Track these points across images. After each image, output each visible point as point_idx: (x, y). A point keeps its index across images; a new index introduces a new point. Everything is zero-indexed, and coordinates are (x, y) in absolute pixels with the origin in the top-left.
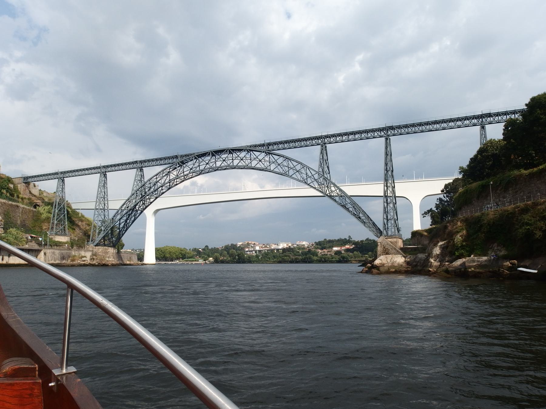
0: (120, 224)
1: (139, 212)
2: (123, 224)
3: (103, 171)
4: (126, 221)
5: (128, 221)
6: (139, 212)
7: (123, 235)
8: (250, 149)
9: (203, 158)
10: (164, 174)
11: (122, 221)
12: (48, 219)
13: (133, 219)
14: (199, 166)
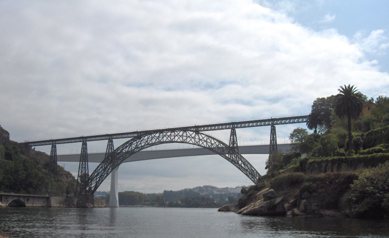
1: (110, 170)
3: (84, 140)
4: (101, 176)
6: (110, 170)
8: (185, 129)
9: (154, 134)
10: (127, 145)
11: (98, 176)
13: (106, 175)
14: (152, 140)
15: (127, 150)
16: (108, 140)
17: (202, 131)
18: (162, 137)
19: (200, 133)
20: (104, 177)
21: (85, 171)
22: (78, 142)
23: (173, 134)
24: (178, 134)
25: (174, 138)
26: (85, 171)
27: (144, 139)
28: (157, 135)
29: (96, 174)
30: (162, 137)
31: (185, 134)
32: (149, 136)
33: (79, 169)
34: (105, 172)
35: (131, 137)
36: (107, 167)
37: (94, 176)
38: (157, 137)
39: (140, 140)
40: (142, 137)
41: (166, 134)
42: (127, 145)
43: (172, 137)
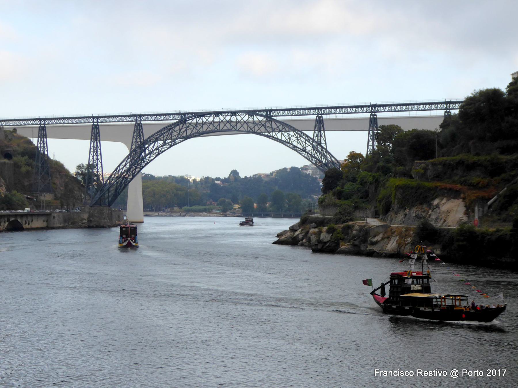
7: (119, 194)
9: (207, 118)
12: (28, 173)
17: (275, 116)
39: (185, 126)
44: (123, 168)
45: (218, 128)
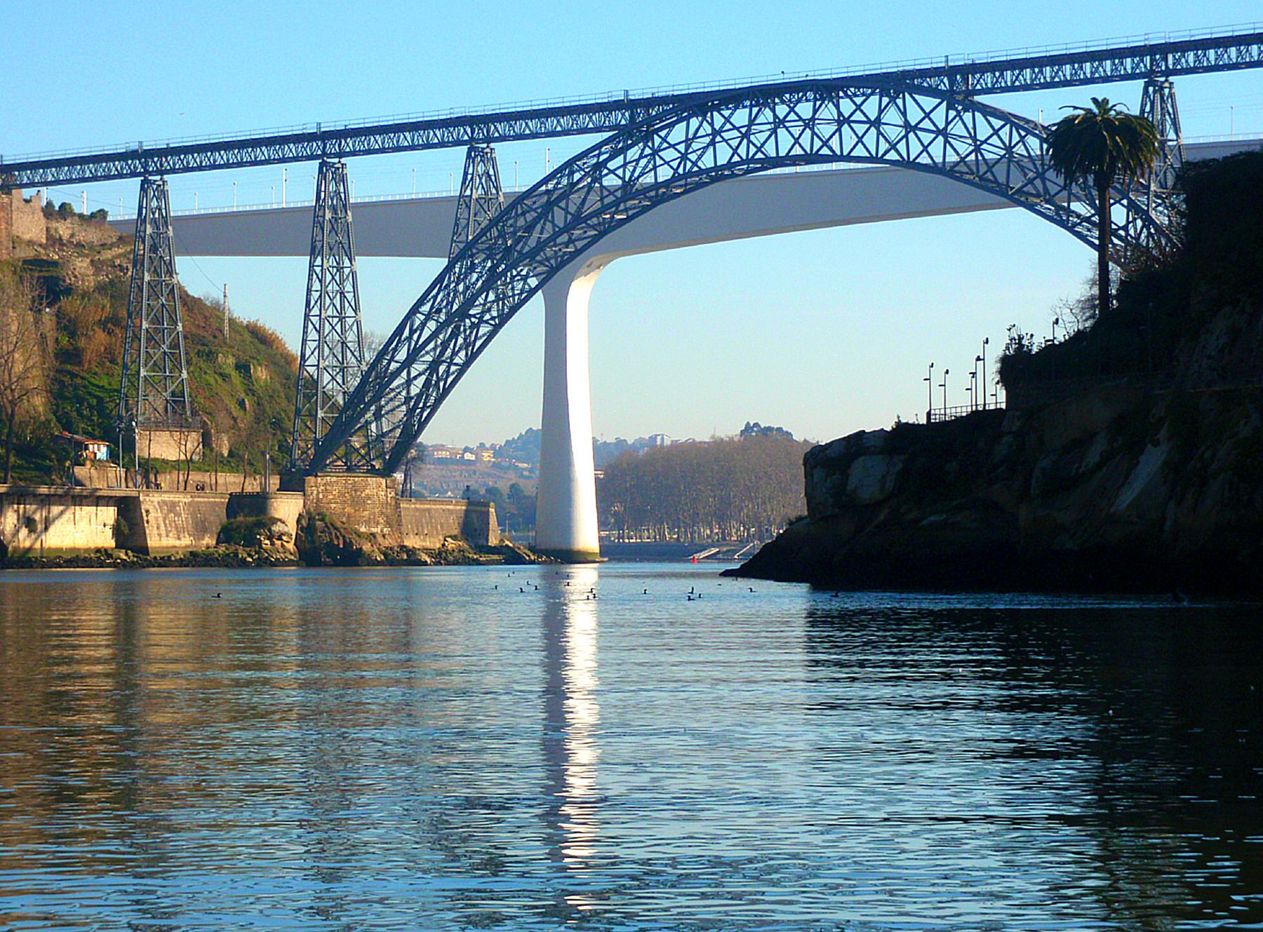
0: (409, 382)
1: (484, 329)
2: (420, 382)
5: (442, 368)
6: (484, 329)
7: (422, 425)
8: (894, 84)
9: (726, 113)
10: (577, 176)
11: (417, 368)
13: (461, 358)
14: (713, 143)
15: (572, 209)
16: (465, 148)
18: (769, 127)
19: (988, 111)
20: (453, 368)
21: (343, 330)
22: (120, 176)
23: (828, 111)
24: (858, 107)
25: (839, 130)
26: (343, 330)
27: (672, 139)
28: (741, 117)
29: (402, 355)
30: (769, 127)
31: (892, 116)
32: (694, 122)
33: (305, 327)
34: (460, 340)
35: (598, 129)
36: (463, 313)
37: (394, 366)
38: (743, 130)
40: (662, 129)
41: (792, 110)
42: (577, 176)
43: (826, 130)
44: (423, 324)
45: (770, 149)
